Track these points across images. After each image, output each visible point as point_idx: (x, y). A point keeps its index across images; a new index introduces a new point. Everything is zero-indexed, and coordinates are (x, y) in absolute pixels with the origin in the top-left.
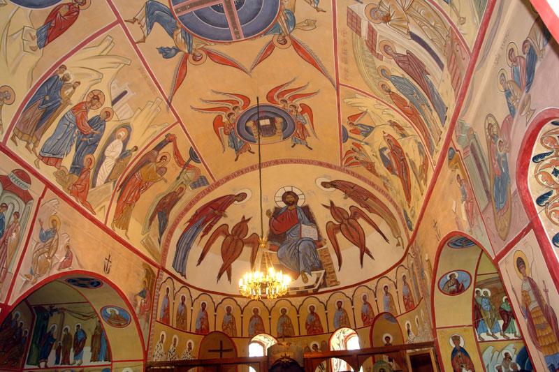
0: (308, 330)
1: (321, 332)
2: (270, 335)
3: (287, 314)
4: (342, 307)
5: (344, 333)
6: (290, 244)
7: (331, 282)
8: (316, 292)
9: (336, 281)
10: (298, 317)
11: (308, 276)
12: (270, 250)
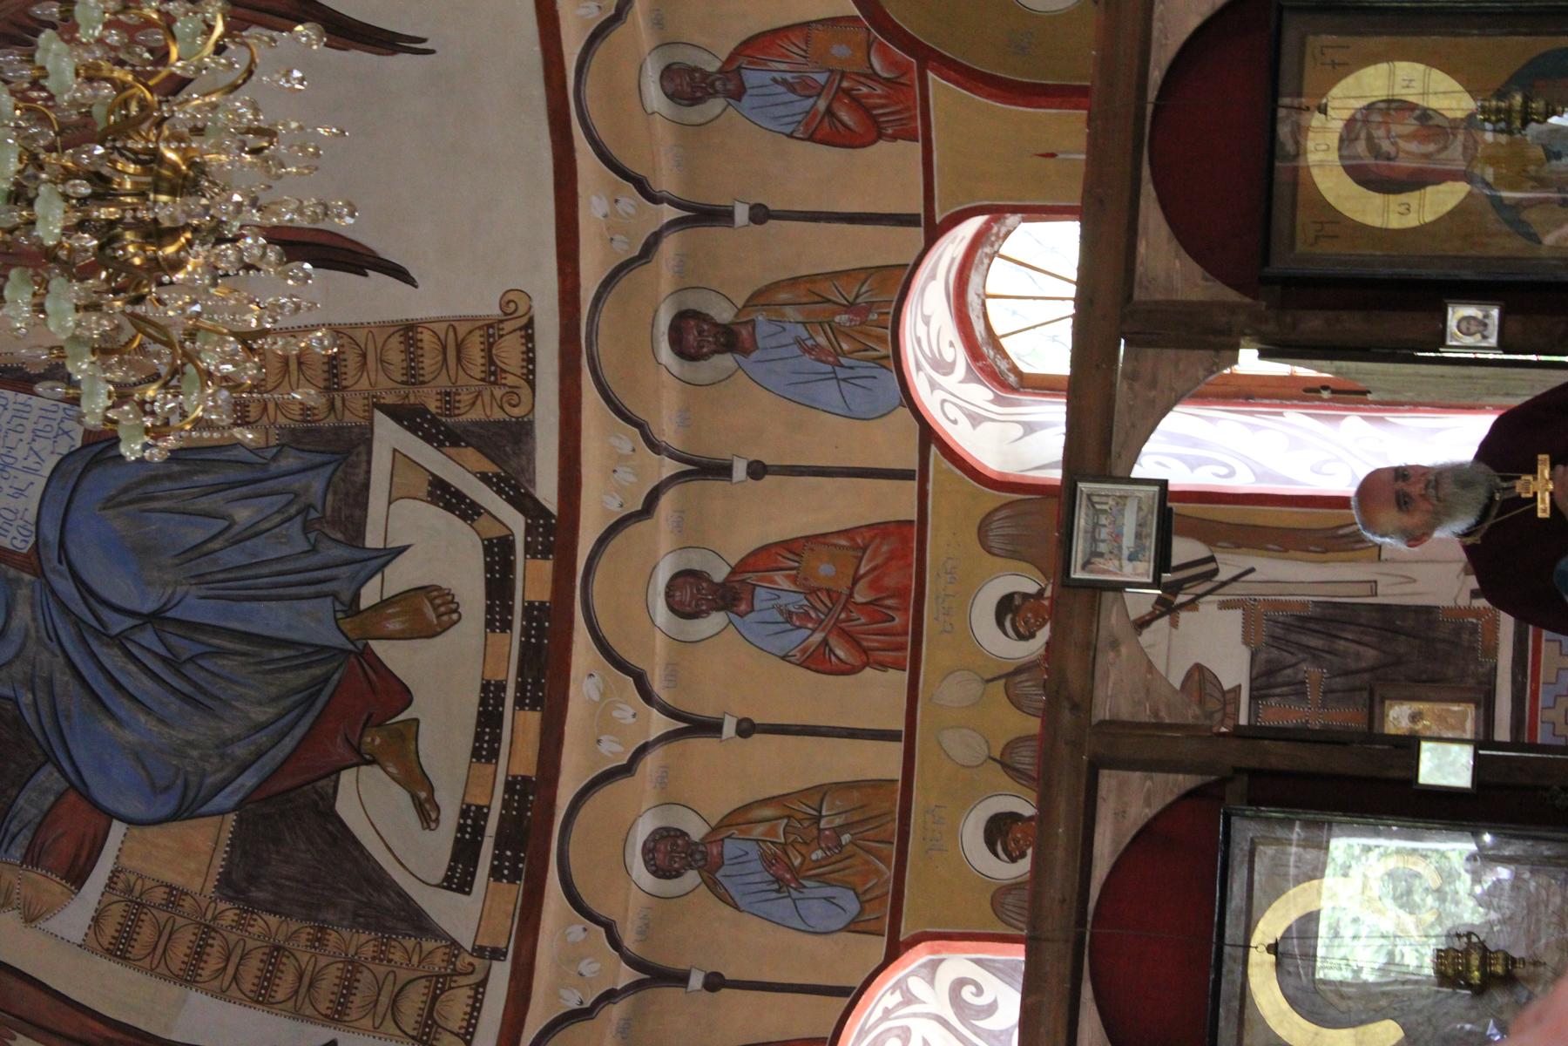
0: (868, 659)
1: (906, 539)
2: (852, 996)
3: (696, 830)
4: (724, 314)
5: (945, 368)
6: (63, 678)
7: (493, 372)
8: (554, 533)
9: (491, 330)
10: (747, 729)
11: (399, 577)
12: (77, 876)
